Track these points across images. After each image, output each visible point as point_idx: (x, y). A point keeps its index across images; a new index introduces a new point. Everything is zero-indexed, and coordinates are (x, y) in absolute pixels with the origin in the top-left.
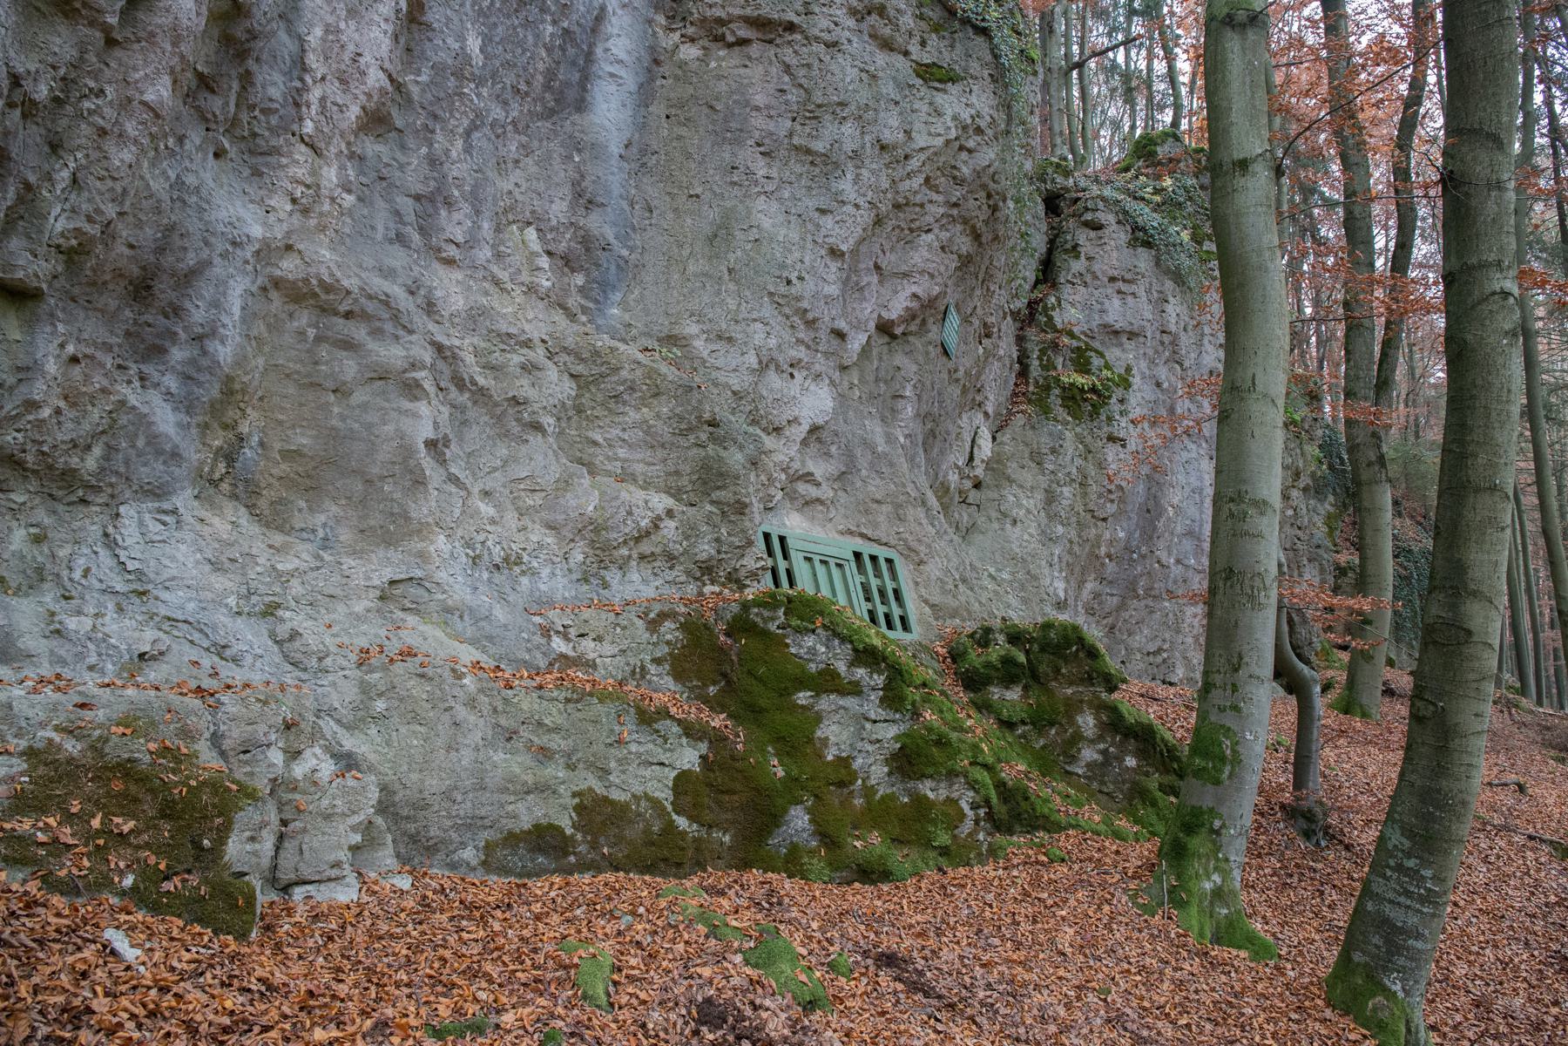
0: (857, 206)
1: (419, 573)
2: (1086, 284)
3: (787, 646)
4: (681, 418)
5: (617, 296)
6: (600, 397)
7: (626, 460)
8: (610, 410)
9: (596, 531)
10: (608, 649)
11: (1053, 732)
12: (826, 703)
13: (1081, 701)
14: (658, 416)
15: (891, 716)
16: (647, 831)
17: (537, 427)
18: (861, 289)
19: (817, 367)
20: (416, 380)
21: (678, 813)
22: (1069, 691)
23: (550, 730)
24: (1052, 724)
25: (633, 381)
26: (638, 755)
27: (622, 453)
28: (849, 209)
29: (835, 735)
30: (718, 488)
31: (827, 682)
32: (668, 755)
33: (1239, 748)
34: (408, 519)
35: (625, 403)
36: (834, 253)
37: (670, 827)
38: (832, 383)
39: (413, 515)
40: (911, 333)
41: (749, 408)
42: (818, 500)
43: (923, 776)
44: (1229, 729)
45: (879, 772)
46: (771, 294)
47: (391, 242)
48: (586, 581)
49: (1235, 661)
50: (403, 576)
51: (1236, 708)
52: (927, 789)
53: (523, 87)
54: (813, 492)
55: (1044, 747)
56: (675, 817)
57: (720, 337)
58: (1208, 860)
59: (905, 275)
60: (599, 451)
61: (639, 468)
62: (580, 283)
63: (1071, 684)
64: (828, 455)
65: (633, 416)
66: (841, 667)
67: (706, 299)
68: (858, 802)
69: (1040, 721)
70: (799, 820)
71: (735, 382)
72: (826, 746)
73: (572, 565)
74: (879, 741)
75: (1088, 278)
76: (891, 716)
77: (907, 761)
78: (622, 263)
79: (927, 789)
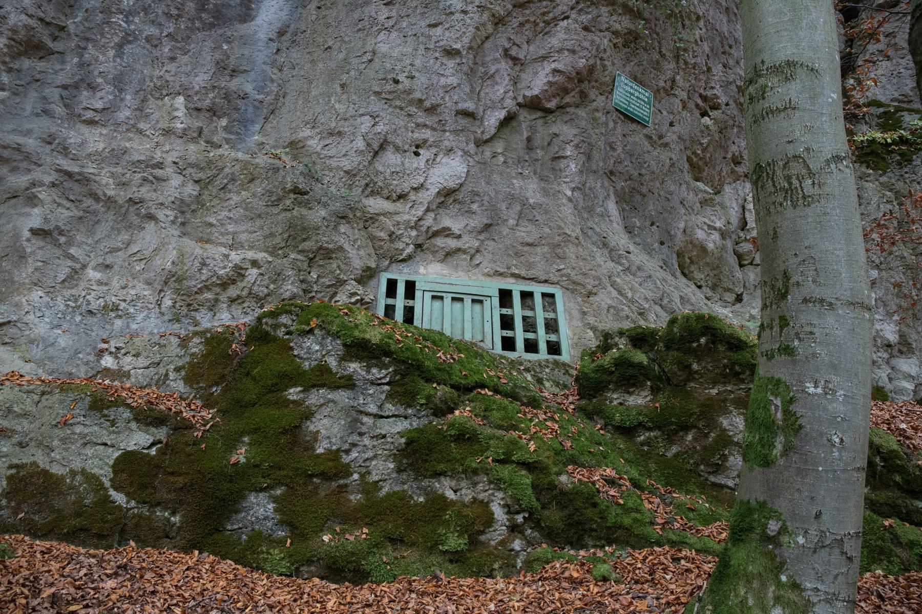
0: (465, 12)
1: (14, 318)
2: (888, 58)
3: (292, 349)
4: (271, 193)
5: (257, 127)
6: (214, 192)
7: (235, 233)
8: (221, 199)
9: (179, 280)
10: (142, 362)
11: (690, 437)
12: (315, 398)
13: (725, 401)
14: (254, 195)
15: (402, 410)
16: (79, 501)
17: (151, 217)
18: (492, 76)
19: (447, 143)
20: (33, 193)
21: (116, 489)
22: (714, 392)
23: (19, 416)
24: (686, 428)
25: (233, 174)
26: (83, 436)
27: (231, 228)
28: (458, 16)
29: (327, 429)
30: (304, 240)
31: (321, 378)
32: (113, 437)
33: (794, 408)
34: (13, 282)
35: (230, 191)
36: (450, 53)
37: (107, 499)
38: (466, 153)
39: (16, 279)
40: (568, 105)
41: (363, 182)
42: (459, 250)
43: (438, 475)
44: (779, 381)
45: (383, 469)
46: (377, 93)
47: (37, 115)
48: (178, 321)
49: (780, 284)
50: (5, 320)
51: (788, 350)
52: (446, 488)
53: (174, 12)
54: (453, 243)
55: (676, 455)
56: (112, 492)
57: (331, 134)
58: (764, 586)
59: (544, 58)
60: (214, 229)
61: (243, 237)
62: (224, 124)
63: (715, 383)
64: (471, 212)
65: (235, 198)
66: (332, 362)
67: (318, 110)
68: (355, 498)
69: (670, 425)
70: (261, 508)
71: (346, 164)
72: (316, 440)
73: (163, 309)
74: (384, 437)
75: (891, 53)
76: (402, 410)
77: (416, 455)
78: (256, 103)
79: (446, 488)
